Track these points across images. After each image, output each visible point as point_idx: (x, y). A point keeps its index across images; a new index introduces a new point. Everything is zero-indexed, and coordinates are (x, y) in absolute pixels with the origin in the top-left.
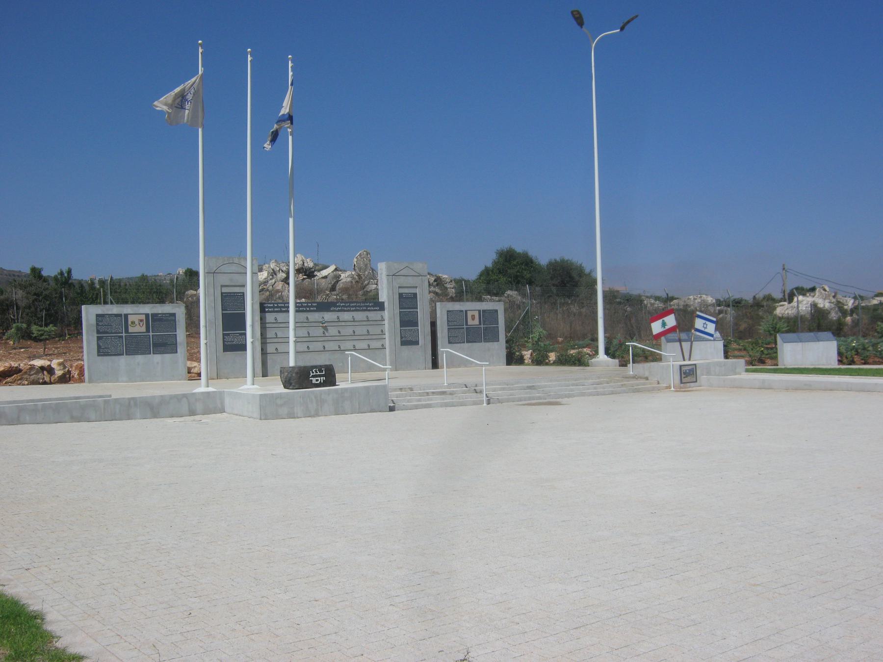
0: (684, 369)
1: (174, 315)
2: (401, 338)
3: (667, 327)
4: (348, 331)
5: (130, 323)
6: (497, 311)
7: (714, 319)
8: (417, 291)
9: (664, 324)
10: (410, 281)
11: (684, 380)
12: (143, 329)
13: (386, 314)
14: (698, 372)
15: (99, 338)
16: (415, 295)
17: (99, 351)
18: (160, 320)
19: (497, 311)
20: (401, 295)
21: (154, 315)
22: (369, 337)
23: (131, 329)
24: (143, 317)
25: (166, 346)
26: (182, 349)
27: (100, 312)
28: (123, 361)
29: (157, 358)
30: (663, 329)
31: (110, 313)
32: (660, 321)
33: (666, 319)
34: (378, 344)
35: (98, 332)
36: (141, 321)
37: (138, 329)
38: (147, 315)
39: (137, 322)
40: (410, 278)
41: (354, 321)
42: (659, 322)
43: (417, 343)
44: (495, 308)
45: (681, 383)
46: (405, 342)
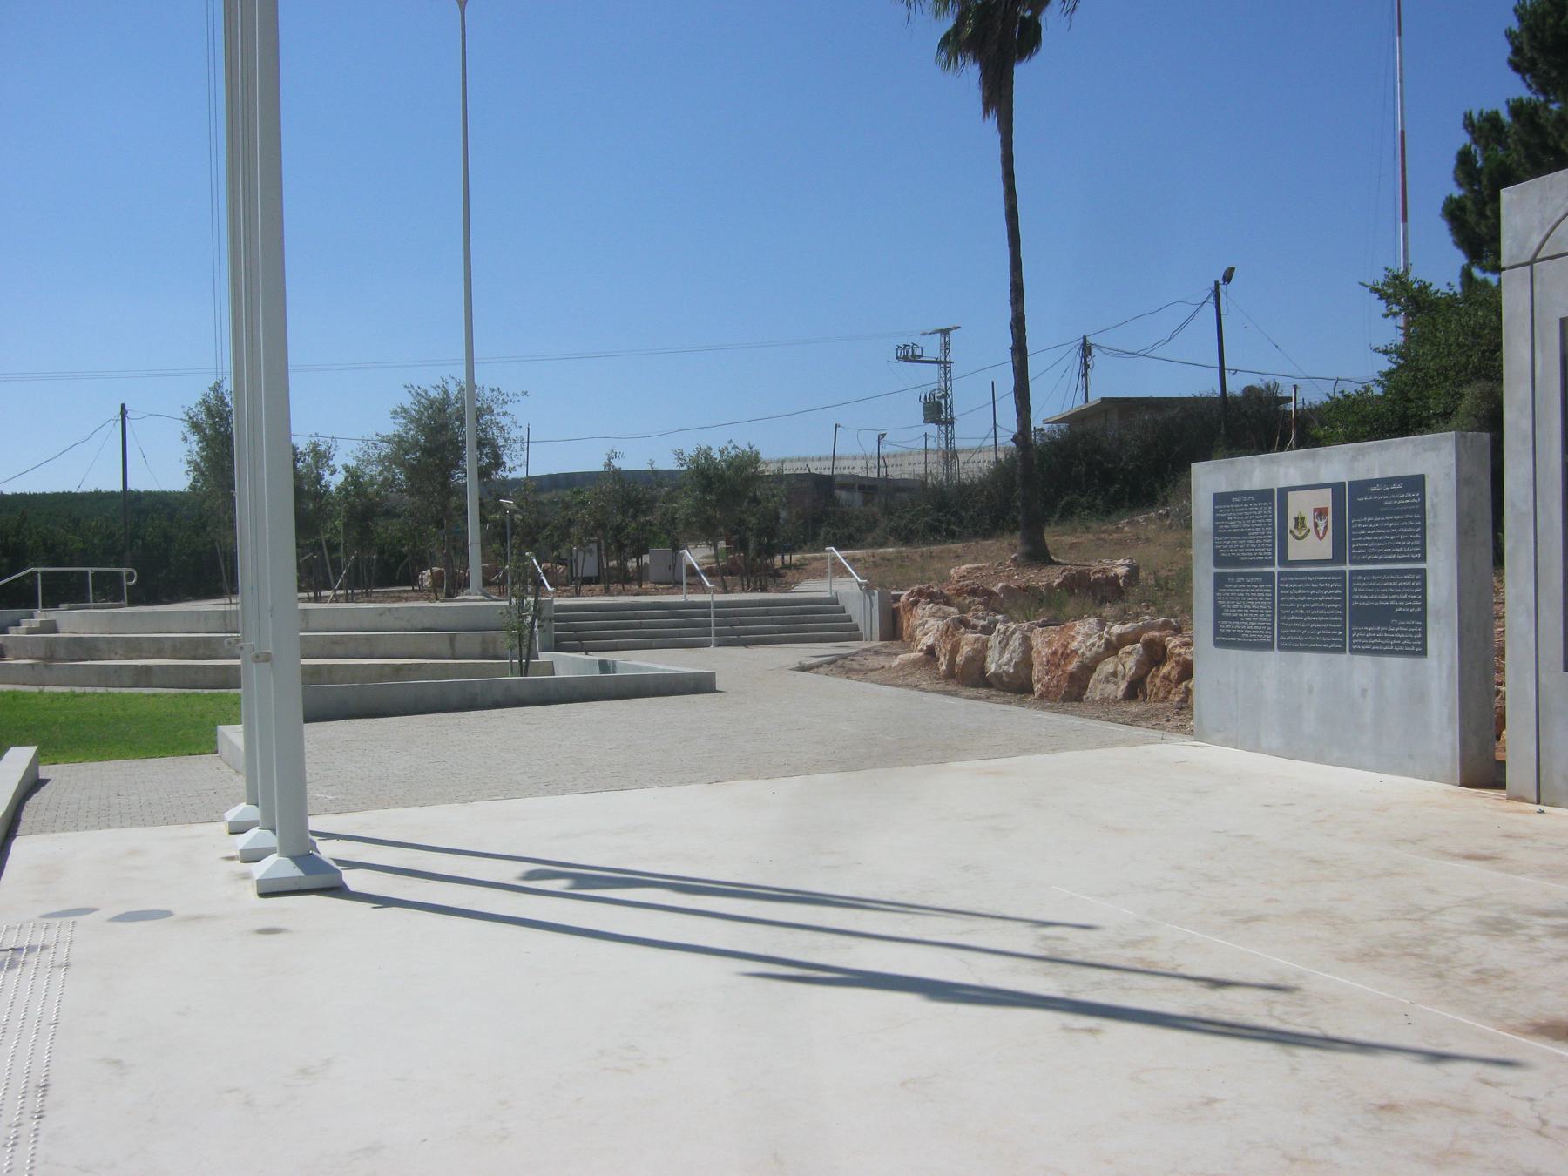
1: (1416, 484)
5: (1291, 524)
12: (1324, 549)
15: (1220, 581)
17: (1217, 632)
18: (1374, 508)
21: (1359, 487)
23: (1296, 550)
24: (1325, 499)
25: (1388, 622)
26: (1442, 637)
27: (1224, 488)
28: (1271, 669)
29: (1359, 670)
31: (1246, 487)
35: (1219, 561)
36: (1321, 513)
37: (1312, 547)
38: (1337, 489)
39: (1309, 524)
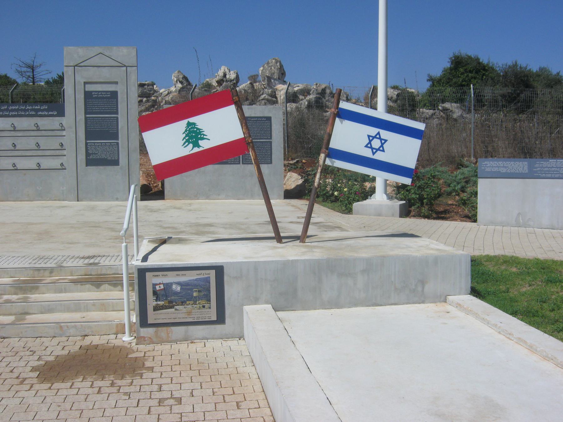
0: (151, 279)
2: (87, 154)
3: (205, 145)
4: (7, 143)
6: (269, 119)
7: (421, 126)
8: (120, 89)
9: (194, 135)
10: (105, 74)
11: (152, 317)
13: (67, 120)
14: (231, 292)
16: (114, 94)
19: (269, 119)
20: (88, 95)
22: (40, 153)
30: (189, 150)
32: (180, 127)
33: (202, 121)
34: (55, 163)
40: (105, 70)
41: (15, 130)
42: (178, 128)
43: (115, 162)
44: (267, 115)
45: (144, 322)
46: (92, 161)
